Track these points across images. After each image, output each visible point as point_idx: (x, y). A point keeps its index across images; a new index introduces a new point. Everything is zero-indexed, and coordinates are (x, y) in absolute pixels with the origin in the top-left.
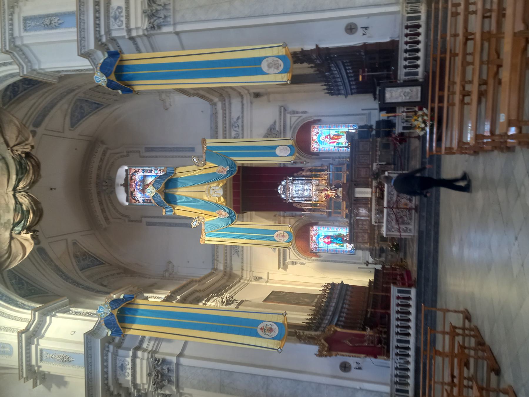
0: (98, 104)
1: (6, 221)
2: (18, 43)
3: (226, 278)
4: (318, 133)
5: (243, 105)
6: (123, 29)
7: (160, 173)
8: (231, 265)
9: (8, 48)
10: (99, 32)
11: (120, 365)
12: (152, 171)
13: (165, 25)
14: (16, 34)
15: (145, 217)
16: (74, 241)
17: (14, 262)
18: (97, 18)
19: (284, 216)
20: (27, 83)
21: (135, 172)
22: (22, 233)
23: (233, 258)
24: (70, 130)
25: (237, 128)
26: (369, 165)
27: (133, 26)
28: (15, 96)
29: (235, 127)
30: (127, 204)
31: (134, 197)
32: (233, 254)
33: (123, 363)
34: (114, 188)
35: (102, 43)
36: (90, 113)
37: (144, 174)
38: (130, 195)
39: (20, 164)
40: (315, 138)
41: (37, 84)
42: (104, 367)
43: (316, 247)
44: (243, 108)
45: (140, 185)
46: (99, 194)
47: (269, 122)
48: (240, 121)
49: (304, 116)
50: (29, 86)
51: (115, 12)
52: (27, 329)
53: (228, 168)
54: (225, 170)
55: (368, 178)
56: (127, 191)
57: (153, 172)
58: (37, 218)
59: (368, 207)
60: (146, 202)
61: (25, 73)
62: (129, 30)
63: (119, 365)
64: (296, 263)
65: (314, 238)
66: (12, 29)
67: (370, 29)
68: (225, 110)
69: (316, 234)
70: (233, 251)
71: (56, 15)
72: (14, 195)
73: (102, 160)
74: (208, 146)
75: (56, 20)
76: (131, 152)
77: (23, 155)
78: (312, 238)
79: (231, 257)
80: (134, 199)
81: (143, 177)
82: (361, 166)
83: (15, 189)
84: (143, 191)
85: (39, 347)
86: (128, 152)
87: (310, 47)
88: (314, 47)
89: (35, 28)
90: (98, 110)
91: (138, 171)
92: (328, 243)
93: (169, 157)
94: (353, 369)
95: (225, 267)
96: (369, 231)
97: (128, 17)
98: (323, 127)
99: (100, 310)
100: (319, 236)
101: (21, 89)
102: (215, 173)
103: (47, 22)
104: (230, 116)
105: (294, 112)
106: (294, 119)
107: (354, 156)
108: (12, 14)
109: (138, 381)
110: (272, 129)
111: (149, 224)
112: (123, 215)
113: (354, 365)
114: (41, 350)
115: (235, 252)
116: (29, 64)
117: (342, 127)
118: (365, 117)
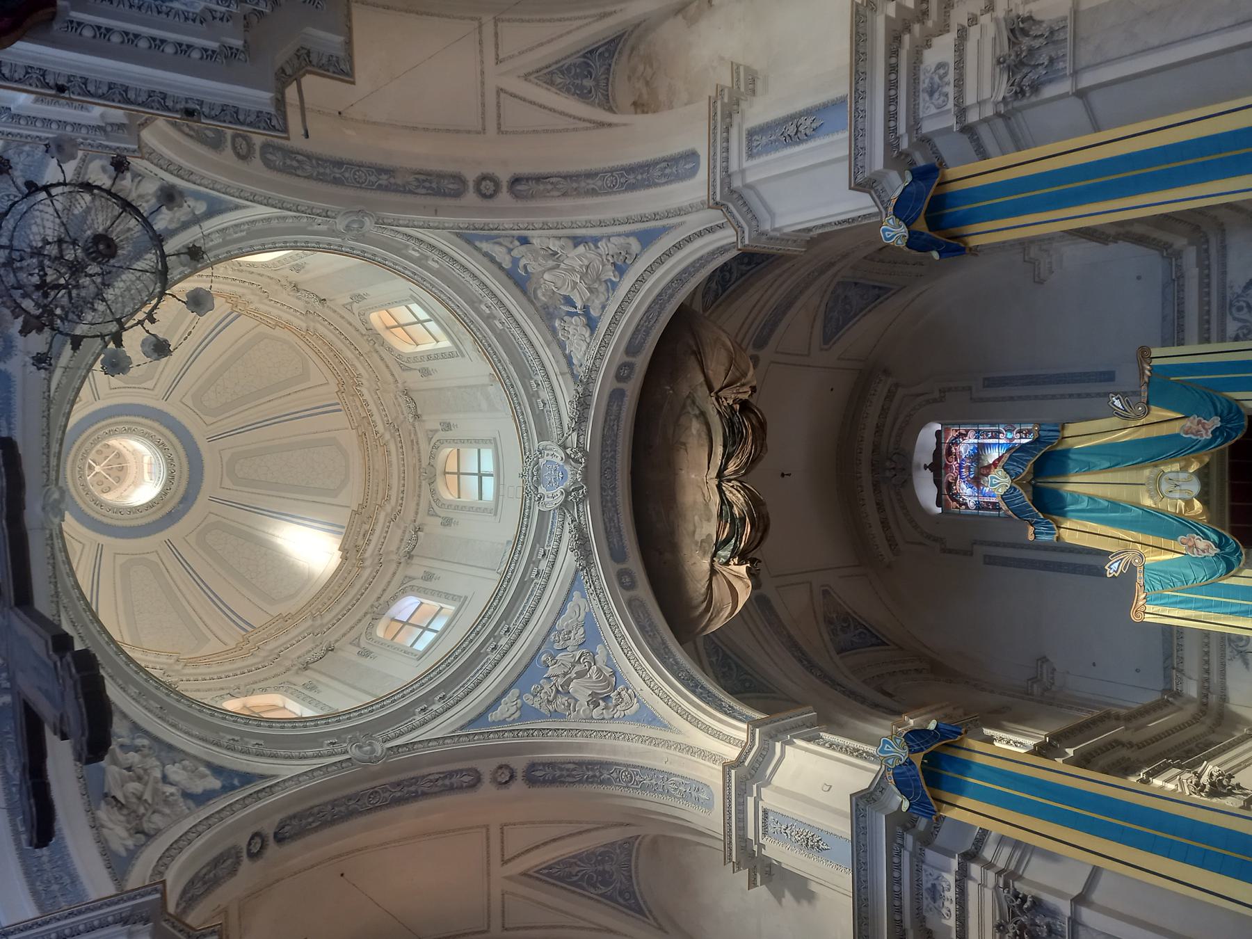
0: (880, 288)
1: (704, 537)
2: (737, 183)
3: (1209, 721)
6: (949, 110)
7: (1021, 438)
8: (1224, 688)
9: (718, 199)
10: (895, 129)
11: (929, 885)
12: (1000, 432)
13: (1050, 81)
14: (734, 167)
15: (983, 543)
16: (827, 588)
17: (716, 620)
18: (891, 100)
20: (746, 260)
21: (958, 437)
22: (732, 563)
24: (822, 350)
27: (970, 99)
28: (724, 291)
29: (1240, 309)
30: (939, 510)
31: (953, 494)
32: (1228, 657)
33: (935, 882)
34: (911, 475)
35: (901, 154)
36: (862, 310)
37: (980, 441)
39: (731, 424)
41: (763, 261)
45: (969, 468)
46: (876, 486)
50: (749, 267)
51: (932, 78)
52: (739, 762)
53: (1216, 422)
54: (1207, 427)
56: (937, 482)
57: (1001, 435)
58: (759, 535)
60: (983, 509)
62: (961, 112)
63: (927, 885)
66: (727, 160)
68: (1208, 267)
70: (1228, 650)
71: (807, 113)
72: (719, 487)
73: (884, 411)
74: (1156, 366)
76: (950, 389)
77: (737, 407)
79: (1223, 665)
80: (954, 500)
81: (977, 449)
83: (720, 475)
84: (976, 482)
90: (879, 301)
91: (966, 435)
93: (1044, 397)
97: (960, 83)
99: (885, 749)
101: (735, 275)
102: (1178, 435)
103: (792, 130)
108: (727, 130)
111: (990, 560)
114: (765, 812)
115: (1236, 653)
116: (754, 223)
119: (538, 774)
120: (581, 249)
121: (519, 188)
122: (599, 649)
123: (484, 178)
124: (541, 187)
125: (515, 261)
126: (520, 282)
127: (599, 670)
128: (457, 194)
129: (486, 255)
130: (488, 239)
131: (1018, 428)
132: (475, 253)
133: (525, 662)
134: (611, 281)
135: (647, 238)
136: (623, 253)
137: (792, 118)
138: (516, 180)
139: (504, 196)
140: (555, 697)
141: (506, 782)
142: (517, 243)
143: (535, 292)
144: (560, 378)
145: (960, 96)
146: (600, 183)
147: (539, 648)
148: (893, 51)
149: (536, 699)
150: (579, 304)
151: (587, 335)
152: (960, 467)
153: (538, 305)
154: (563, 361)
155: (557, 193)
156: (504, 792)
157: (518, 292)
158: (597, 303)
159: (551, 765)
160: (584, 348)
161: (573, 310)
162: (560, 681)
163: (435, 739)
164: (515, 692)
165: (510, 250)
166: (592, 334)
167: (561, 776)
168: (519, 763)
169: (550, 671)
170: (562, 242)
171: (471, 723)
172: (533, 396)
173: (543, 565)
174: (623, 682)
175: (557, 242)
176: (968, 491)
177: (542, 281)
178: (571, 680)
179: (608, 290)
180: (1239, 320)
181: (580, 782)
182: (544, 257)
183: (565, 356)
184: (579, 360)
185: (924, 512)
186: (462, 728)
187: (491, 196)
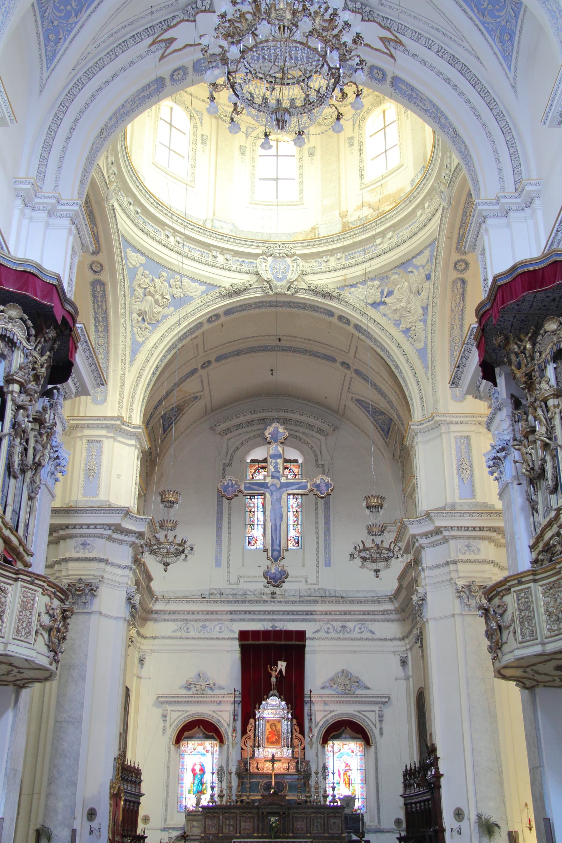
0: (388, 432)
2: (443, 428)
3: (144, 615)
4: (353, 752)
5: (391, 640)
6: (458, 557)
8: (161, 620)
9: (436, 418)
11: (88, 542)
14: (453, 427)
19: (234, 702)
25: (359, 631)
26: (310, 833)
27: (460, 566)
29: (360, 628)
30: (249, 461)
36: (376, 421)
42: (88, 526)
43: (189, 751)
44: (386, 639)
47: (366, 680)
49: (376, 732)
52: (123, 423)
55: (293, 833)
59: (254, 833)
61: (412, 427)
64: (165, 721)
65: (202, 747)
66: (457, 423)
67: (459, 836)
69: (207, 751)
71: (472, 475)
75: (467, 476)
78: (201, 744)
79: (173, 620)
82: (309, 821)
85: (104, 439)
86: (323, 466)
87: (442, 767)
92: (193, 771)
93: (317, 528)
94: (90, 823)
95: (157, 612)
96: (221, 835)
97: (469, 562)
98: (361, 759)
103: (465, 466)
104: (375, 620)
105: (381, 717)
106: (371, 716)
107: (322, 810)
109: (71, 565)
110: (357, 684)
112: (232, 456)
114: (100, 442)
116: (422, 431)
117: (362, 788)
118: (376, 823)
119: (98, 287)
120: (421, 311)
121: (459, 283)
122: (172, 309)
123: (467, 264)
124: (458, 297)
125: (416, 267)
127: (159, 312)
128: (458, 249)
129: (422, 252)
130: (431, 256)
131: (299, 510)
132: (423, 246)
133: (162, 262)
134: (400, 324)
135: (422, 353)
136: (415, 337)
137: (471, 465)
138: (463, 282)
139: (454, 275)
140: (142, 288)
141: (92, 269)
142: (427, 273)
143: (399, 274)
144: (341, 278)
145: (462, 561)
146: (456, 333)
147: (170, 269)
148: (489, 529)
149: (140, 276)
150: (387, 300)
151: (369, 301)
153: (389, 273)
154: (353, 282)
155: (453, 305)
156: (87, 268)
157: (399, 263)
158: (388, 312)
159: (104, 295)
160: (361, 298)
162: (152, 289)
163: (117, 227)
164: (143, 260)
165: (423, 267)
166: (369, 304)
167: (98, 301)
168: (104, 277)
169: (157, 281)
170: (425, 301)
171: (126, 240)
172: (332, 252)
173: (221, 259)
175: (425, 298)
177: (403, 280)
178: (153, 296)
179: (395, 320)
180: (354, 628)
181: (95, 313)
182: (418, 287)
183: (356, 283)
184: (353, 292)
186: (123, 236)
187: (455, 267)
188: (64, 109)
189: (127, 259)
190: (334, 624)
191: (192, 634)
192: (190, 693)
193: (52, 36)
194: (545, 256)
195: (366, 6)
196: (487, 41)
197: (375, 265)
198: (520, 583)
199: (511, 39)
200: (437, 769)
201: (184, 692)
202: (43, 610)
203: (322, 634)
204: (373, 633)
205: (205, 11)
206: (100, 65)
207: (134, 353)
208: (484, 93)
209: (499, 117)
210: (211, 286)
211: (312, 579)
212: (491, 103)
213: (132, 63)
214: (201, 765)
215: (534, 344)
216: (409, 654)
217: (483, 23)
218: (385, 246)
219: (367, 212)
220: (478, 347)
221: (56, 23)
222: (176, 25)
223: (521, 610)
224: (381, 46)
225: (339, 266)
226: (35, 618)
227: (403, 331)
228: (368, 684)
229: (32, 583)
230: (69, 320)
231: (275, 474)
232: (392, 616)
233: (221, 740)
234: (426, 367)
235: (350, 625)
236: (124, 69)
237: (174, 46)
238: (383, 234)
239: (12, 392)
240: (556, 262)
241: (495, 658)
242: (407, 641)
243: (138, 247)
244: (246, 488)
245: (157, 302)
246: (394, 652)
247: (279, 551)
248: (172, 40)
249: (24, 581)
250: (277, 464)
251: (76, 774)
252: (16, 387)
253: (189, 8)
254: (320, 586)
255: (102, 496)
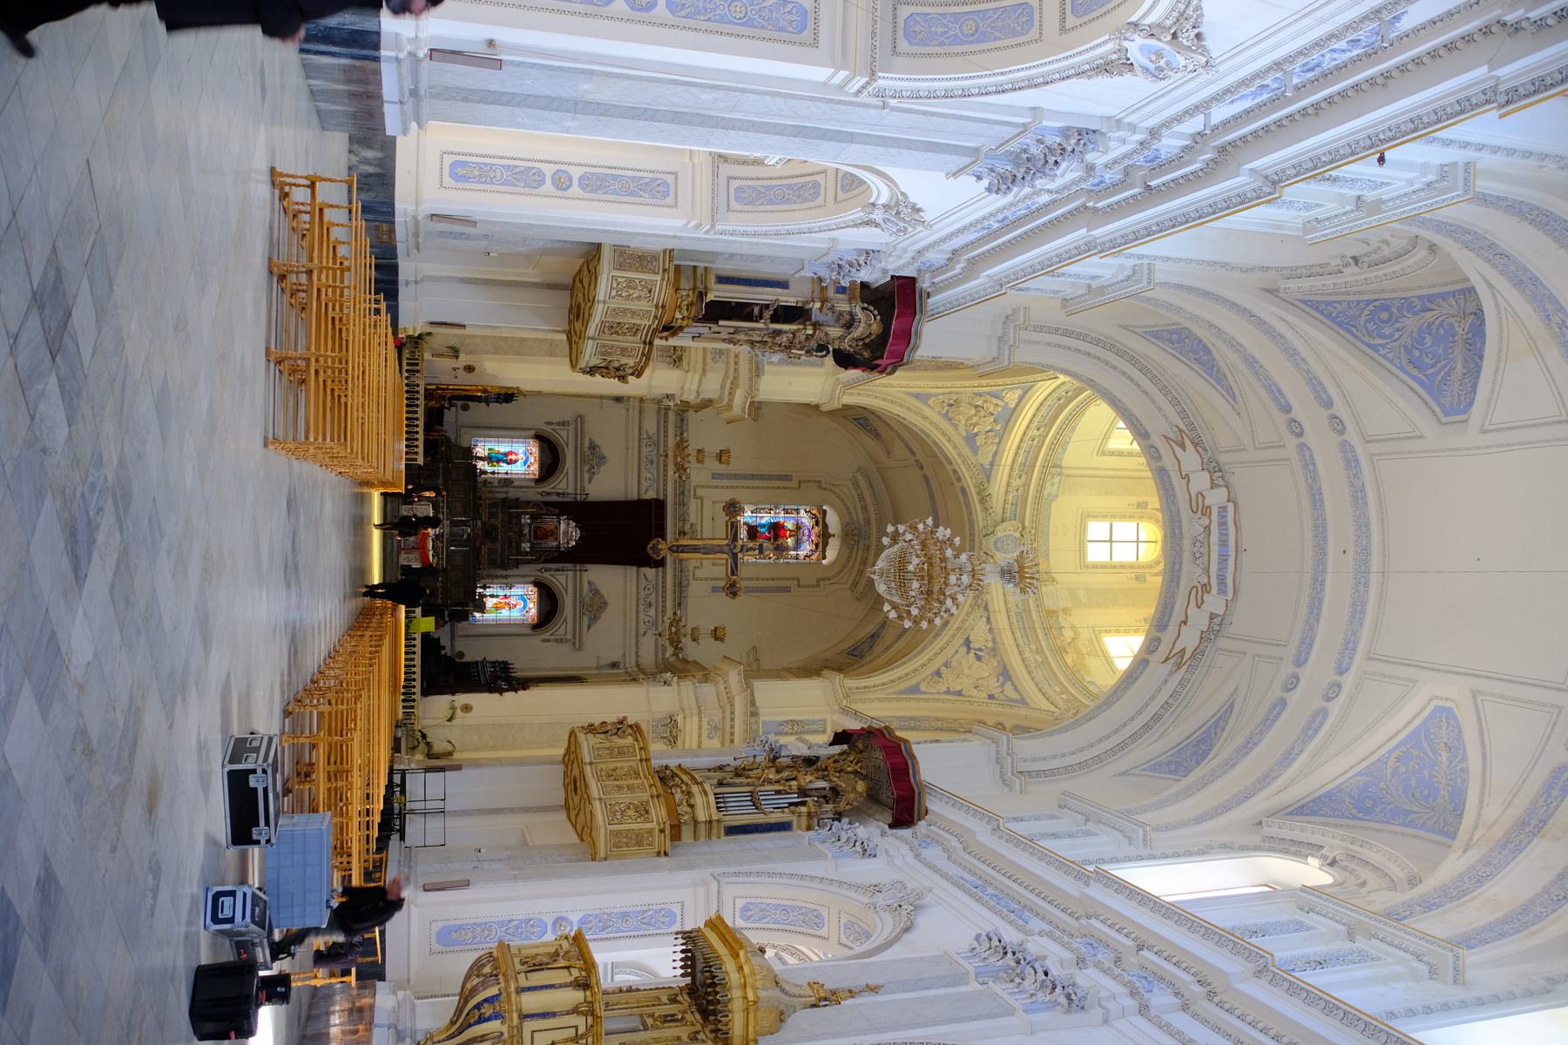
23: (655, 428)
27: (696, 719)
34: (843, 531)
38: (820, 520)
40: (531, 605)
46: (868, 522)
48: (642, 630)
49: (546, 636)
56: (825, 526)
64: (558, 424)
65: (532, 460)
70: (655, 439)
76: (813, 586)
79: (658, 430)
80: (815, 515)
84: (798, 527)
86: (818, 586)
87: (509, 695)
88: (505, 694)
89: (814, 722)
92: (511, 453)
97: (700, 728)
98: (520, 620)
100: (525, 462)
105: (560, 641)
106: (561, 631)
111: (788, 478)
113: (461, 372)
117: (493, 620)
118: (460, 633)
125: (1002, 685)
126: (1005, 674)
130: (1012, 700)
133: (1010, 424)
134: (946, 667)
135: (915, 689)
144: (997, 609)
145: (700, 719)
150: (972, 654)
152: (809, 536)
154: (992, 620)
157: (1008, 667)
158: (959, 655)
161: (978, 653)
162: (982, 413)
171: (1030, 389)
174: (943, 415)
175: (972, 694)
176: (804, 520)
178: (975, 415)
185: (833, 506)
188: (1108, 347)
189: (1011, 389)
190: (653, 595)
191: (645, 450)
192: (586, 450)
193: (1175, 337)
194: (920, 784)
195: (1216, 636)
196: (1171, 749)
197: (1007, 640)
198: (641, 749)
199: (1171, 772)
200: (507, 690)
201: (587, 443)
202: (623, 363)
203: (643, 583)
204: (644, 634)
205: (1212, 480)
206: (1154, 379)
207: (917, 396)
208: (1123, 746)
209: (1097, 759)
210: (988, 473)
211: (699, 573)
212: (1111, 752)
213: (1160, 409)
214: (516, 461)
215: (851, 773)
216: (622, 671)
217: (1187, 746)
218: (1028, 655)
219: (1068, 634)
220: (862, 729)
221: (1187, 340)
222: (1197, 451)
223: (618, 748)
224: (1178, 648)
225: (1009, 606)
226: (615, 358)
227: (939, 670)
228: (596, 627)
229: (643, 354)
230: (879, 369)
231: (745, 549)
232: (660, 655)
233: (537, 481)
234: (900, 693)
235: (652, 612)
236: (1154, 402)
237: (1178, 450)
238: (1040, 651)
239: (805, 329)
240: (913, 791)
241: (583, 728)
242: (635, 669)
243: (1024, 401)
244: (732, 523)
245: (970, 418)
246: (624, 655)
247: (677, 552)
248: (1183, 447)
249: (644, 348)
250: (754, 550)
251: (505, 353)
252: (810, 332)
253: (1214, 464)
254: (691, 582)
255: (767, 368)
